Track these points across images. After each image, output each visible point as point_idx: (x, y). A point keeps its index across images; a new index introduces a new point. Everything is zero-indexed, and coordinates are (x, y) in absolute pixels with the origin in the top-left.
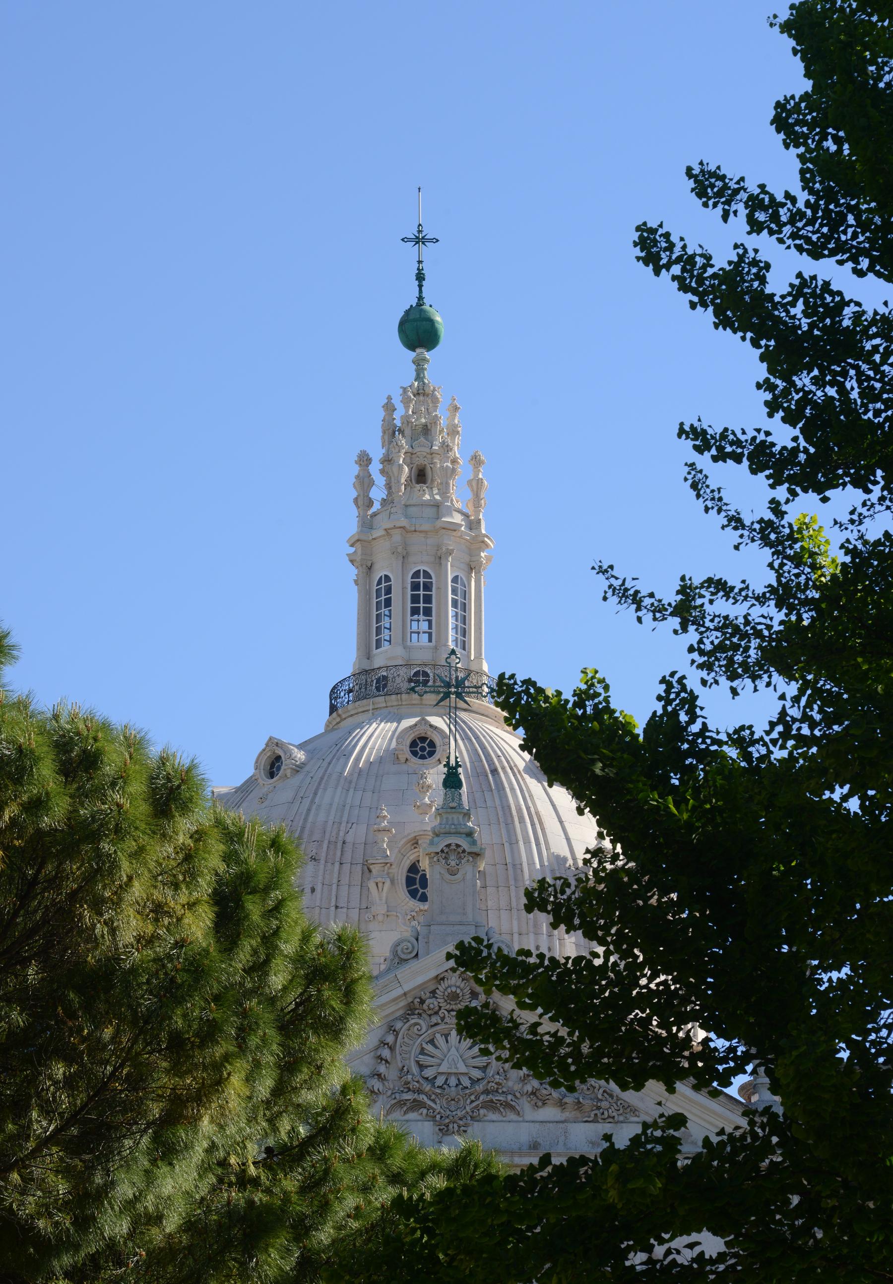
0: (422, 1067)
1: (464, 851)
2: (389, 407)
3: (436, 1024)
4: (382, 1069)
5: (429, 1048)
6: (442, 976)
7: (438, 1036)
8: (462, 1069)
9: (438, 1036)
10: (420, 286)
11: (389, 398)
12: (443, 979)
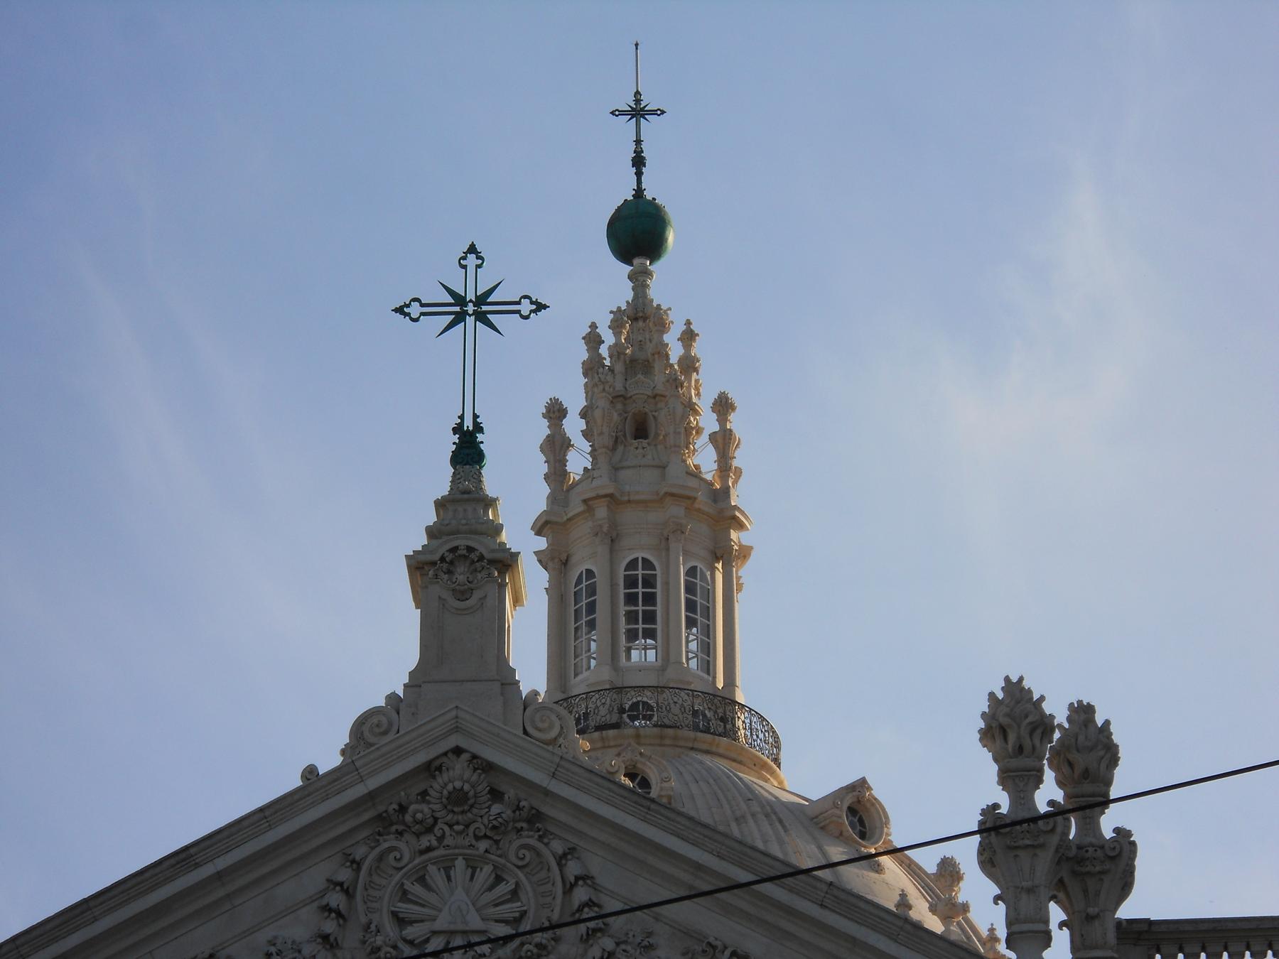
0: (401, 921)
1: (481, 558)
2: (593, 340)
3: (429, 849)
4: (330, 926)
5: (417, 889)
6: (437, 763)
7: (432, 869)
8: (475, 922)
9: (432, 869)
10: (639, 174)
11: (593, 326)
12: (439, 769)
